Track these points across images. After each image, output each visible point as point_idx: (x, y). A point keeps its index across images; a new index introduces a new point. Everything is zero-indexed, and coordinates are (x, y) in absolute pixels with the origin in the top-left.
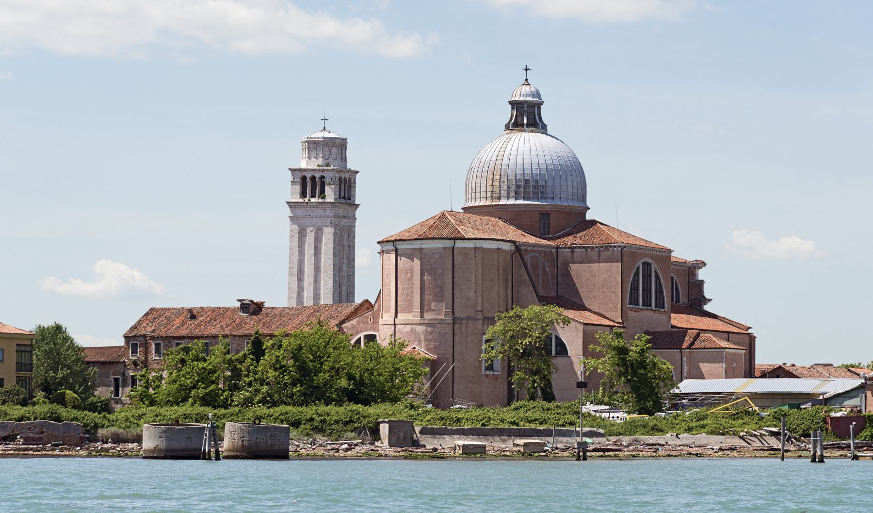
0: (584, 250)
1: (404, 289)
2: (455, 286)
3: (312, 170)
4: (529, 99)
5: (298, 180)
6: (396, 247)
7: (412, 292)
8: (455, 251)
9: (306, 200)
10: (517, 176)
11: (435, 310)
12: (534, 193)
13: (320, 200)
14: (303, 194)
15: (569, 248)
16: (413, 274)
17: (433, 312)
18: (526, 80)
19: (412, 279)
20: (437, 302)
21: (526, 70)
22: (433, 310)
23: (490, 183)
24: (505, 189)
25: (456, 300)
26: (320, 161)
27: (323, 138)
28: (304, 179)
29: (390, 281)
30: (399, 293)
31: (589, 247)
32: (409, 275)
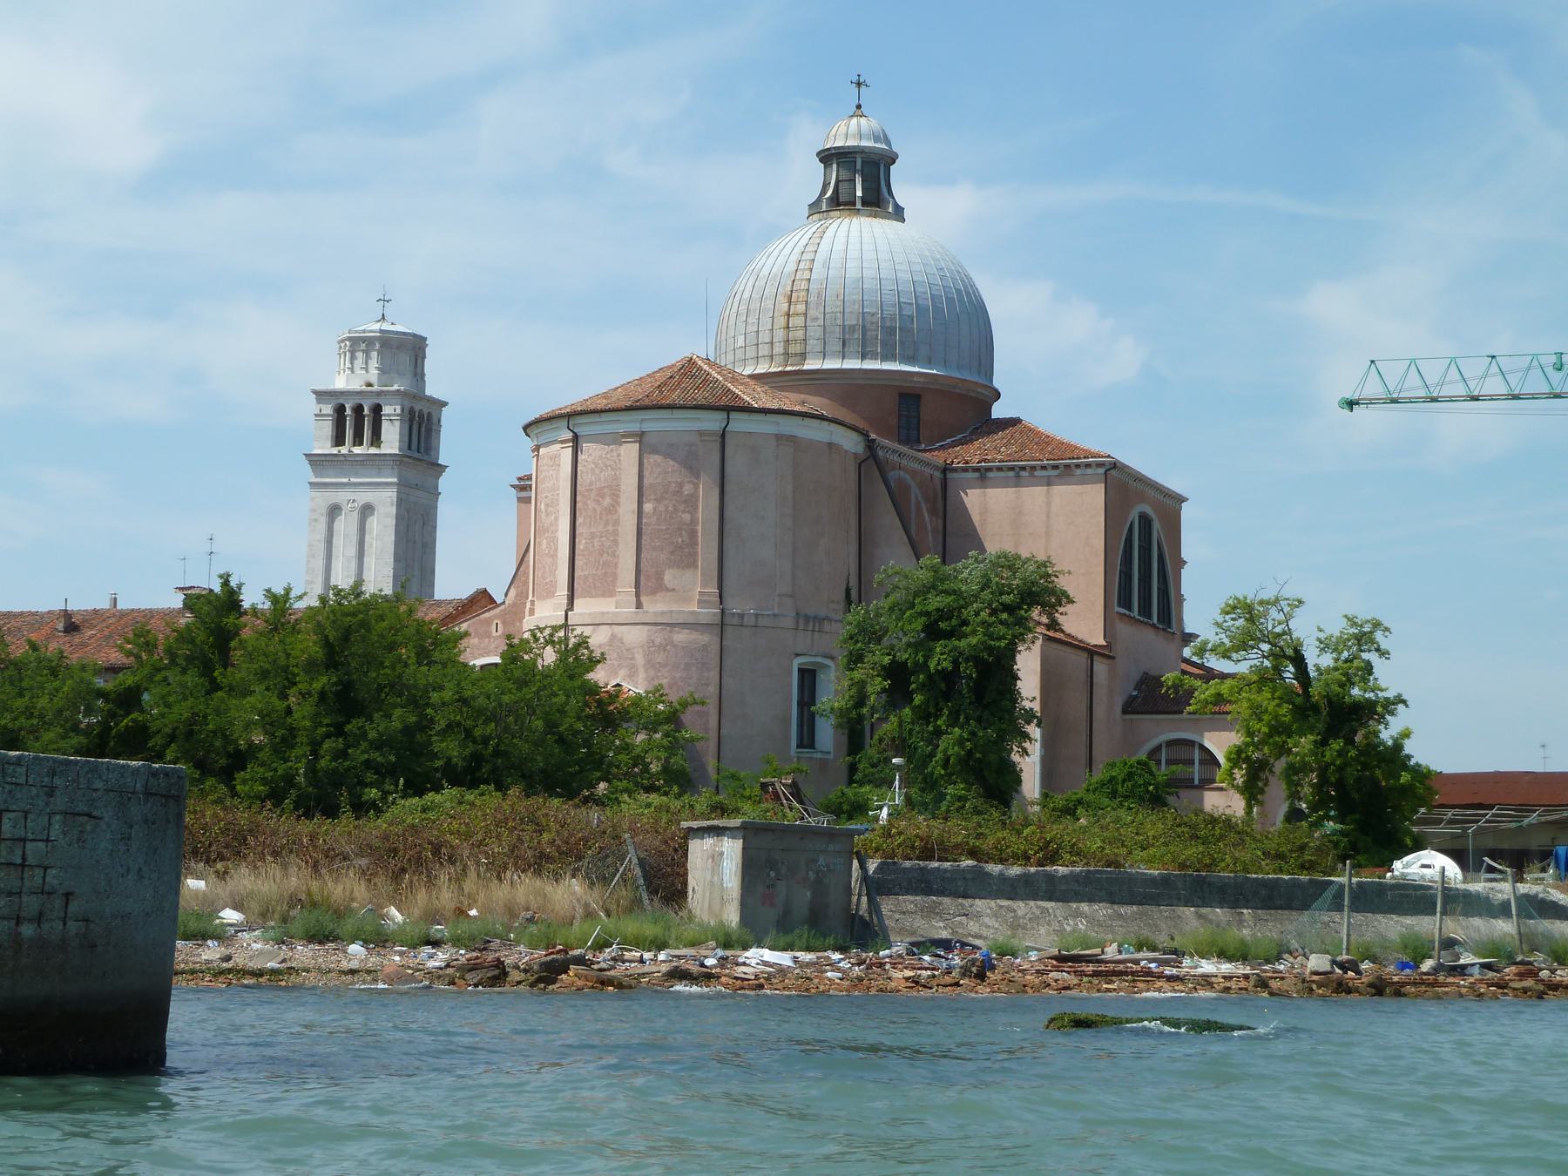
0: (1011, 474)
1: (593, 536)
2: (726, 529)
3: (358, 393)
4: (864, 143)
5: (328, 409)
6: (575, 431)
7: (616, 542)
8: (729, 439)
9: (344, 450)
10: (846, 305)
11: (673, 590)
12: (884, 344)
13: (373, 450)
14: (339, 440)
15: (976, 470)
16: (618, 496)
17: (669, 594)
18: (859, 107)
19: (616, 511)
20: (678, 567)
21: (859, 84)
22: (668, 590)
23: (782, 321)
24: (817, 336)
25: (728, 563)
26: (373, 374)
27: (381, 331)
28: (340, 410)
29: (556, 519)
30: (580, 546)
31: (1023, 468)
32: (607, 501)
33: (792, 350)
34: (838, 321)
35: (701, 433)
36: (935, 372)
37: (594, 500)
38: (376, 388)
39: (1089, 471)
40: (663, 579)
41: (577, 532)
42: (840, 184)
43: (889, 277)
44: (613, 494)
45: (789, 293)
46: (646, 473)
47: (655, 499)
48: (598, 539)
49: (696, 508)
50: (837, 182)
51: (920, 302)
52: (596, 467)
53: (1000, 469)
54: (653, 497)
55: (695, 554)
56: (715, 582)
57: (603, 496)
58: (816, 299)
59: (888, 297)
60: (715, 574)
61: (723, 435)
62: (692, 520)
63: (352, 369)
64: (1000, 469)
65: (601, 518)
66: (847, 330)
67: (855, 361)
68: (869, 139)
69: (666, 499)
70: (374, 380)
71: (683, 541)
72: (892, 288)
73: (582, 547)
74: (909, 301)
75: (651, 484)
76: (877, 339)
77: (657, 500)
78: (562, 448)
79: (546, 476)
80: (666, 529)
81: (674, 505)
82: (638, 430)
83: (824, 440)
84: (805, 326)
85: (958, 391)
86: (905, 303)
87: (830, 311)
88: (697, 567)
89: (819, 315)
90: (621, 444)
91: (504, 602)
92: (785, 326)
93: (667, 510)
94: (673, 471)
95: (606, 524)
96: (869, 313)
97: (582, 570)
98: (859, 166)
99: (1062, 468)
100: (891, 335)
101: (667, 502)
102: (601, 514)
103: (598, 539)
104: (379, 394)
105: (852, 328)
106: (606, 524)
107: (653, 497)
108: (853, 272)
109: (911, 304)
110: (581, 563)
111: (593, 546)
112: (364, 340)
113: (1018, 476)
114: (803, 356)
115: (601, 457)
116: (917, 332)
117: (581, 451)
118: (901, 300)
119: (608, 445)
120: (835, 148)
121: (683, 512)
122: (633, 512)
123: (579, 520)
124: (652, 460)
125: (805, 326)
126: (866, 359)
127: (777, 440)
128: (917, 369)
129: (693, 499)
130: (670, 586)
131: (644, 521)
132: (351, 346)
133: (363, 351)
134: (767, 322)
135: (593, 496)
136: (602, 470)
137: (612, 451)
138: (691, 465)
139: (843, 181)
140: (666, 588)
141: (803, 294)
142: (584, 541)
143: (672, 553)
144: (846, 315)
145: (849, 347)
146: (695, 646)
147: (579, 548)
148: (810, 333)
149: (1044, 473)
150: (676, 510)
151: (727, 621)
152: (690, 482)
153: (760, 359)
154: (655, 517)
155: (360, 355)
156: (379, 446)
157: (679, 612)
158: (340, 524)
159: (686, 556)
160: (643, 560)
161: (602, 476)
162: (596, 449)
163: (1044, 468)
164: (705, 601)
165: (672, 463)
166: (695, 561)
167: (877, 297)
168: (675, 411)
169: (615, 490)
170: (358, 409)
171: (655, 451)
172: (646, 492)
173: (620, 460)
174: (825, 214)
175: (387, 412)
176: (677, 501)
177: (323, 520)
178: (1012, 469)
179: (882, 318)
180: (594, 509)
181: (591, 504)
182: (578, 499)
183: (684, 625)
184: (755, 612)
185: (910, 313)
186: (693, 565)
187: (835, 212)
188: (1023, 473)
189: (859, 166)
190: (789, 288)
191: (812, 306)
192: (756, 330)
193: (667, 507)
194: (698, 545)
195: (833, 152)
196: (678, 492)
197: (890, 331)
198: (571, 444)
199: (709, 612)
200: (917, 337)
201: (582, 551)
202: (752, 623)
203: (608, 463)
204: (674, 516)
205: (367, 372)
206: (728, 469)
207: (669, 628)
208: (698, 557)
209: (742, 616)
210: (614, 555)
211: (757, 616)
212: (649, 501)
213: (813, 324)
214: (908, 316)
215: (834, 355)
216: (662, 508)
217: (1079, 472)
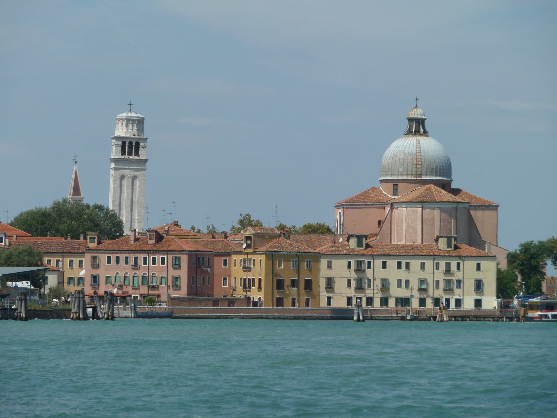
0: (474, 207)
3: (131, 138)
6: (423, 205)
8: (457, 209)
9: (126, 157)
13: (137, 158)
14: (123, 153)
18: (417, 105)
23: (415, 166)
26: (135, 131)
27: (138, 117)
30: (424, 232)
31: (477, 206)
32: (432, 222)
33: (418, 173)
35: (452, 208)
38: (136, 137)
39: (493, 207)
61: (456, 209)
63: (127, 129)
70: (136, 134)
90: (435, 210)
91: (376, 239)
104: (139, 139)
105: (433, 169)
112: (131, 120)
113: (475, 208)
114: (421, 175)
117: (424, 210)
121: (449, 225)
123: (424, 226)
124: (442, 214)
125: (422, 168)
128: (445, 179)
132: (126, 122)
133: (131, 124)
138: (450, 215)
141: (420, 159)
149: (482, 207)
155: (130, 125)
156: (139, 156)
158: (125, 182)
163: (482, 206)
170: (131, 143)
175: (141, 145)
177: (119, 180)
178: (474, 206)
188: (477, 207)
191: (423, 163)
197: (440, 169)
205: (133, 131)
215: (429, 175)
217: (490, 207)
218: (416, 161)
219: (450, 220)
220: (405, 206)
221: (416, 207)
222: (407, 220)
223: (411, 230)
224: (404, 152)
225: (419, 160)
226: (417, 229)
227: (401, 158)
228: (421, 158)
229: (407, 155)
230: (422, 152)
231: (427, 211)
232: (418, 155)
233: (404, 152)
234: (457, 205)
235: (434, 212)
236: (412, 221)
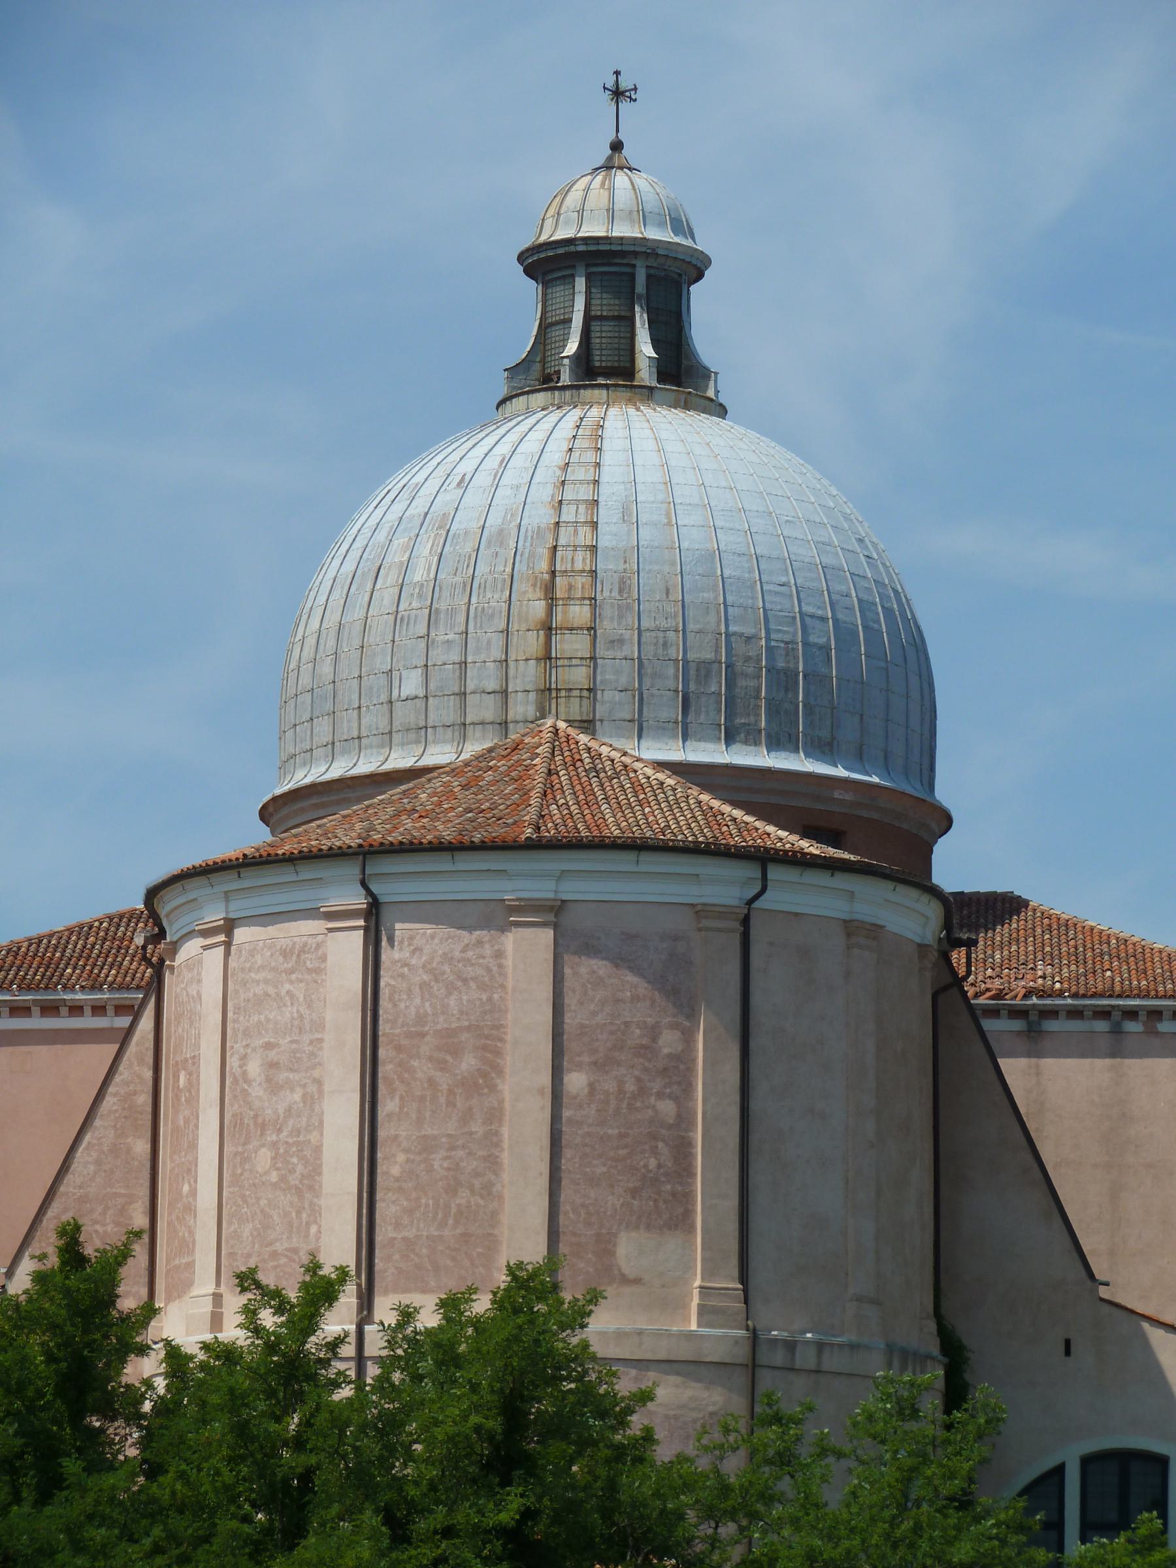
0: (1102, 1026)
1: (427, 1146)
2: (754, 1139)
4: (654, 234)
6: (375, 888)
7: (493, 1163)
10: (690, 613)
11: (638, 1281)
12: (774, 710)
15: (1017, 1013)
16: (498, 1053)
17: (627, 1290)
18: (617, 146)
19: (493, 1088)
20: (648, 1227)
21: (618, 94)
23: (533, 643)
24: (623, 681)
25: (758, 1223)
29: (312, 1101)
30: (391, 1167)
31: (1131, 1014)
32: (468, 1063)
34: (672, 653)
35: (700, 911)
36: (875, 779)
37: (430, 1059)
40: (611, 1253)
41: (382, 1134)
42: (595, 327)
43: (775, 554)
44: (485, 1048)
45: (546, 577)
46: (570, 1000)
47: (595, 1063)
48: (443, 1153)
49: (688, 1088)
50: (588, 319)
51: (840, 616)
52: (437, 981)
53: (1075, 1013)
54: (586, 1059)
55: (687, 1197)
56: (732, 1265)
57: (456, 1051)
58: (615, 594)
59: (778, 599)
60: (733, 1245)
61: (746, 921)
62: (679, 1116)
64: (1075, 1013)
65: (451, 1104)
66: (692, 672)
67: (671, 743)
68: (661, 224)
69: (619, 1064)
71: (659, 1166)
72: (784, 579)
73: (395, 1171)
74: (820, 612)
75: (582, 1026)
76: (758, 697)
77: (599, 1066)
78: (331, 930)
79: (267, 995)
80: (622, 1136)
81: (638, 1080)
82: (551, 895)
83: (910, 935)
84: (593, 658)
85: (905, 826)
86: (812, 616)
87: (652, 625)
88: (691, 1229)
89: (627, 634)
90: (504, 928)
92: (541, 654)
93: (621, 1091)
94: (635, 999)
95: (467, 1116)
96: (741, 635)
97: (398, 1225)
98: (640, 286)
99: (1143, 1016)
100: (787, 690)
101: (623, 1070)
102: (451, 1092)
103: (443, 1153)
105: (705, 669)
106: (467, 1116)
107: (586, 1059)
108: (694, 539)
109: (824, 619)
110: (393, 1209)
111: (430, 1170)
113: (1117, 1031)
115: (447, 958)
116: (838, 685)
117: (391, 940)
118: (805, 608)
119: (470, 929)
120: (586, 240)
121: (660, 1095)
122: (541, 1092)
123: (387, 1106)
125: (593, 658)
126: (734, 742)
127: (849, 935)
128: (840, 772)
129: (682, 1067)
130: (629, 1270)
131: (566, 1113)
134: (489, 642)
135: (425, 1049)
136: (450, 988)
137: (480, 943)
139: (601, 318)
140: (623, 1275)
141: (581, 581)
142: (401, 1157)
143: (634, 1192)
144: (690, 637)
145: (698, 713)
146: (694, 1415)
147: (386, 1173)
148: (606, 673)
150: (642, 1091)
151: (764, 1357)
152: (674, 1026)
153: (470, 729)
154: (593, 1106)
157: (659, 1334)
159: (665, 1202)
160: (565, 1207)
161: (452, 1002)
162: (433, 937)
164: (715, 1311)
165: (631, 978)
166: (688, 1214)
167: (754, 598)
168: (646, 857)
169: (487, 1037)
171: (590, 948)
172: (571, 1045)
173: (500, 966)
174: (568, 393)
176: (646, 1070)
178: (1103, 1014)
179: (769, 649)
180: (431, 1082)
181: (422, 1068)
182: (382, 1053)
183: (669, 1365)
184: (818, 1337)
185: (822, 641)
186: (682, 1222)
187: (596, 392)
188: (1131, 1026)
189: (640, 286)
190: (544, 566)
191: (607, 611)
192: (423, 663)
193: (621, 1083)
194: (694, 1175)
195: (581, 248)
196: (647, 1050)
197: (784, 680)
198: (361, 923)
199: (724, 1337)
200: (839, 696)
201: (397, 1180)
202: (811, 1364)
203: (470, 971)
204: (639, 1104)
206: (756, 998)
207: (633, 1372)
208: (694, 1204)
209: (791, 1346)
210: (488, 1191)
211: (820, 1346)
212: (579, 1067)
213: (610, 654)
214: (821, 647)
215: (664, 730)
216: (610, 1086)
218: (540, 594)
219: (669, 1042)
220: (214, 915)
221: (312, 913)
222: (233, 1062)
223: (263, 1158)
224: (445, 525)
225: (571, 587)
226: (318, 1149)
227: (417, 578)
228: (593, 573)
229: (469, 547)
230: (607, 515)
231: (417, 950)
232: (562, 541)
233: (445, 525)
234: (757, 888)
235: (499, 955)
236: (273, 1065)
